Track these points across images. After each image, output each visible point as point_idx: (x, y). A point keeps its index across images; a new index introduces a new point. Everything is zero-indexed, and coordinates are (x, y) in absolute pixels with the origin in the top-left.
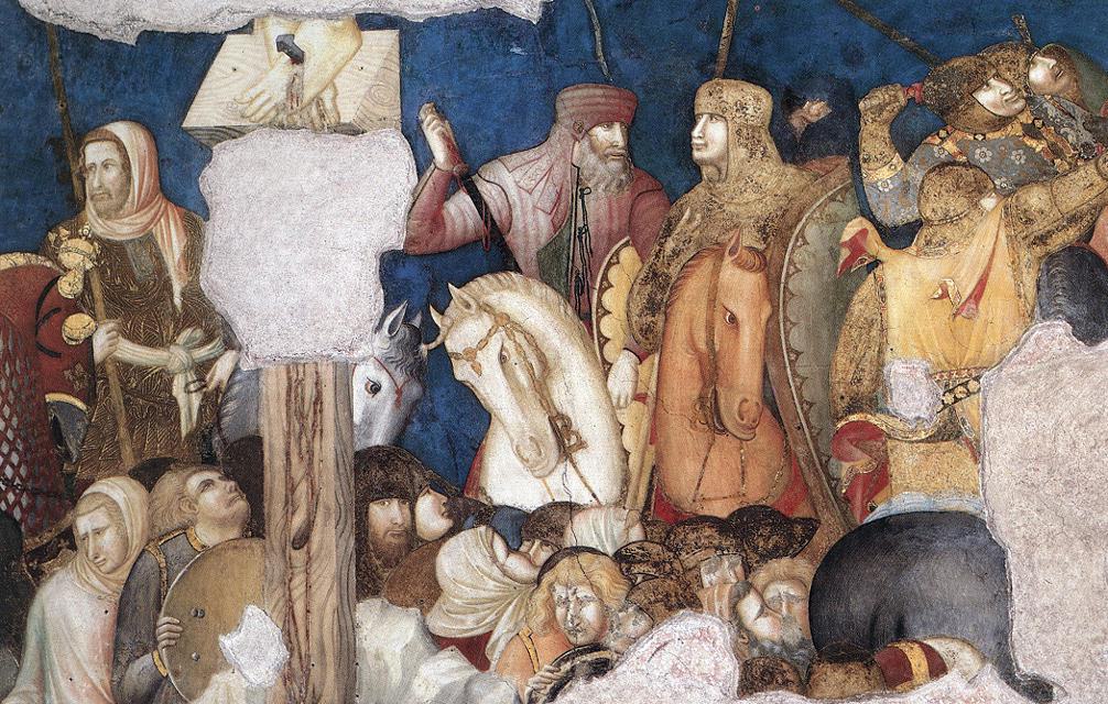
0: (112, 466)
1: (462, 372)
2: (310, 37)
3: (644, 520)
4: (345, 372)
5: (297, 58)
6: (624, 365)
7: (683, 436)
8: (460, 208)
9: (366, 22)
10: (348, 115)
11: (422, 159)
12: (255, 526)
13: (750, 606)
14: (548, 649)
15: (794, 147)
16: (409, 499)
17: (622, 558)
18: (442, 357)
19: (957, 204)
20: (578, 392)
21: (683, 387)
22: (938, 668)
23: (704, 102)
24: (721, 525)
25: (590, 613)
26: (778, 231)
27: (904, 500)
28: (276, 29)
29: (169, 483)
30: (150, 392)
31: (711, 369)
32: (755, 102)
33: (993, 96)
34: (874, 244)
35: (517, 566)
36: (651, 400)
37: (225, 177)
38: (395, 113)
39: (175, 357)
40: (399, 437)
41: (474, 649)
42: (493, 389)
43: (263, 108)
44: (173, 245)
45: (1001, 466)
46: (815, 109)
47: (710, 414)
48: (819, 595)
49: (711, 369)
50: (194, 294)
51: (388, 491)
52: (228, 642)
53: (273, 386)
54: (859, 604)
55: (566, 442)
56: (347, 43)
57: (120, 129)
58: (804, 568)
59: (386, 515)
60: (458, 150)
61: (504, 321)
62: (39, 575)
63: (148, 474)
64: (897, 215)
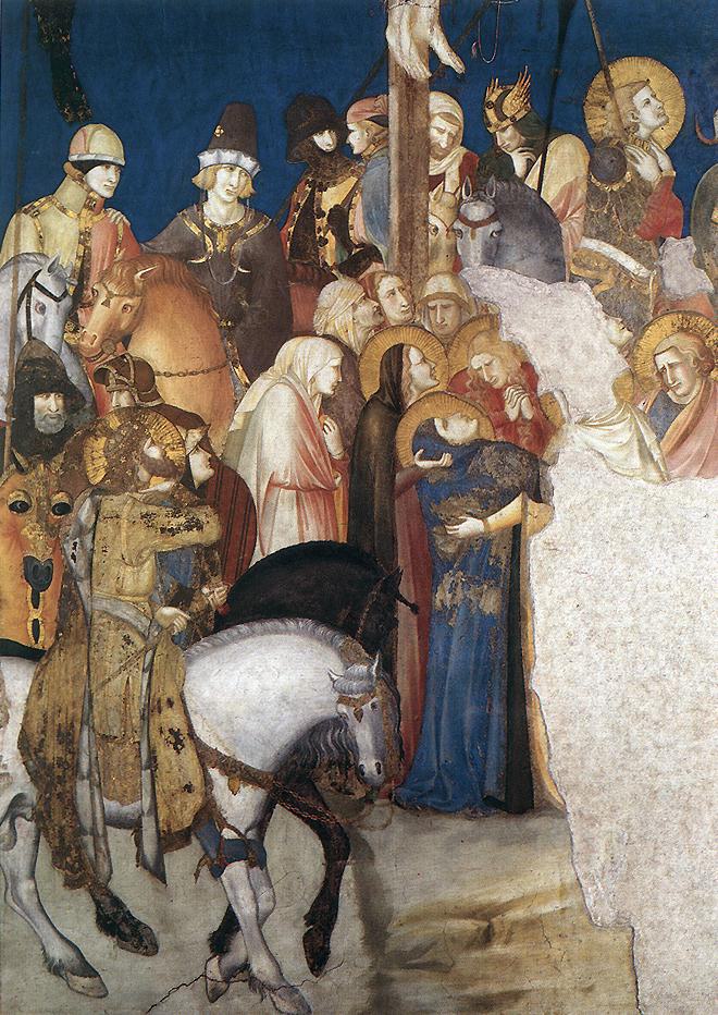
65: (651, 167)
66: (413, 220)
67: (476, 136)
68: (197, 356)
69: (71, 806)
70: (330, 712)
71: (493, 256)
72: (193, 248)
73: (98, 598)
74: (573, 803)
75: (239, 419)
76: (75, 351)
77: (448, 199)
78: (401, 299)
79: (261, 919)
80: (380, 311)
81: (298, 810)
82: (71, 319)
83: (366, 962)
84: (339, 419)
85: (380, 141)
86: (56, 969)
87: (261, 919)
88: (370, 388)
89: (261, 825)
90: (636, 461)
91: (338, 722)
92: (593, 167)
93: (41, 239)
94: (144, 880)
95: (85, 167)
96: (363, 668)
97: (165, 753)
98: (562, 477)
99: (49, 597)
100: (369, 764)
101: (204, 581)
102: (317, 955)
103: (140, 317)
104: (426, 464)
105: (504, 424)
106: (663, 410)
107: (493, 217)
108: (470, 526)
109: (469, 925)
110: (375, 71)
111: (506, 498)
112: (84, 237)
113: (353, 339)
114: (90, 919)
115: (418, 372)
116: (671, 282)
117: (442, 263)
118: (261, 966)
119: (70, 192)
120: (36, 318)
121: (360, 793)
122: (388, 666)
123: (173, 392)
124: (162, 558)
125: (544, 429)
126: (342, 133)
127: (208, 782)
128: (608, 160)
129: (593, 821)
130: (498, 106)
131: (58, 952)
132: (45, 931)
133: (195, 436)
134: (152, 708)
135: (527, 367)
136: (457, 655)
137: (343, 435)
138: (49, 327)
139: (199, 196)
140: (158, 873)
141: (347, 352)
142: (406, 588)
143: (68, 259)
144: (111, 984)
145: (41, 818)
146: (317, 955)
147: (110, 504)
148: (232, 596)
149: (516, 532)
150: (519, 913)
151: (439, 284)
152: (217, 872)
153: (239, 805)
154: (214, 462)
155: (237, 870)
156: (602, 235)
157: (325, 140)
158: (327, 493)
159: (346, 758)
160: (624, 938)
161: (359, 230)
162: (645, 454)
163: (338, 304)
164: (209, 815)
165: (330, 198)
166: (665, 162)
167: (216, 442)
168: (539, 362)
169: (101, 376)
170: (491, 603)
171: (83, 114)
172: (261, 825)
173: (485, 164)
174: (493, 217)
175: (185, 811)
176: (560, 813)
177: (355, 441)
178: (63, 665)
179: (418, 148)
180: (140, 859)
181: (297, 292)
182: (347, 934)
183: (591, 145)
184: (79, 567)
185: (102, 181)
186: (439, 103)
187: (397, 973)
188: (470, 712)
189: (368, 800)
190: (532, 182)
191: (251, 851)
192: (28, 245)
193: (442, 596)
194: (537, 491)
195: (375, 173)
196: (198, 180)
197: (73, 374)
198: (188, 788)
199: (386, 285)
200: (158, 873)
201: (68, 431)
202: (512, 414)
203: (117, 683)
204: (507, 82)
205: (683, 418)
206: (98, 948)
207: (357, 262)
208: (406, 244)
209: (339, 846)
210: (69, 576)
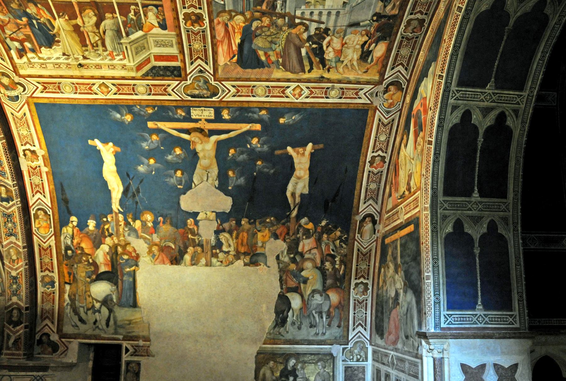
0: (191, 246)
1: (221, 240)
2: (208, 213)
3: (236, 252)
4: (211, 240)
5: (207, 214)
6: (235, 241)
7: (240, 246)
8: (221, 227)
9: (213, 212)
10: (211, 219)
11: (218, 223)
12: (203, 251)
13: (245, 260)
14: (228, 262)
15: (250, 224)
16: (216, 250)
17: (234, 255)
18: (219, 239)
19: (264, 229)
20: (231, 242)
21: (240, 241)
22: (260, 265)
23: (242, 219)
24: (242, 253)
25: (231, 259)
26: (248, 231)
27: (258, 252)
28: (205, 212)
29: (196, 248)
30: (194, 240)
31: (242, 241)
32: (247, 220)
33: (268, 220)
34: (257, 232)
35: (225, 256)
36: (237, 243)
37: (200, 223)
38: (215, 219)
39: (196, 238)
40: (215, 245)
41: (221, 262)
42: (223, 241)
43: (203, 218)
44: (196, 229)
45: (267, 249)
46: (252, 221)
47: (242, 244)
48: (251, 259)
49: (242, 241)
50: (198, 233)
51: (214, 249)
52: (201, 260)
53: (205, 241)
54: (254, 260)
55: (230, 246)
56: (211, 213)
57: (191, 219)
58: (250, 257)
59: (214, 251)
60: (221, 222)
61: (224, 236)
62: (184, 255)
63: (194, 247)
64: (259, 229)
65: (150, 224)
66: (118, 231)
67: (125, 219)
68: (90, 247)
69: (75, 304)
70: (109, 293)
71: (129, 235)
72: (87, 233)
73: (78, 277)
74: (142, 306)
75: (95, 255)
76: (73, 245)
77: (122, 228)
78: (117, 240)
79: (100, 320)
80: (114, 241)
81: (105, 306)
82: (72, 242)
83: (114, 326)
84: (109, 255)
85: (112, 220)
86: (73, 326)
87: (100, 320)
88: (113, 251)
89: (100, 308)
90: (150, 262)
91: (110, 295)
92: (142, 224)
93: (67, 231)
94: (85, 315)
95: (72, 222)
96: (114, 288)
97: (87, 298)
98: (140, 264)
99: (72, 276)
100: (115, 300)
101: (92, 275)
102: (107, 325)
103: (81, 241)
104: (121, 261)
105: (132, 256)
106: (154, 256)
107: (129, 230)
108: (128, 270)
109: (128, 322)
110: (111, 211)
111: (132, 266)
112: (73, 231)
113: (111, 245)
114: (77, 319)
115: (120, 249)
116: (154, 239)
117: (122, 236)
118: (100, 326)
119: (70, 225)
120: (67, 241)
121: (113, 304)
122: (117, 287)
123: (87, 251)
124: (86, 272)
125: (138, 256)
126: (107, 218)
127: (93, 302)
128: (144, 224)
129: (145, 309)
130: (128, 216)
131: (73, 324)
132: (72, 321)
133: (90, 257)
134: (86, 292)
135: (134, 249)
136: (126, 286)
137: (110, 257)
138: (69, 242)
139: (88, 226)
140: (86, 313)
141: (110, 246)
142: (120, 277)
143: (71, 233)
144: (80, 328)
145: (71, 306)
146: (107, 325)
147: (79, 265)
148: (96, 278)
149: (134, 271)
150: (134, 321)
151: (122, 238)
152: (94, 314)
153: (97, 305)
154: (93, 260)
155: (97, 314)
156: (144, 233)
157: (105, 219)
158: (108, 265)
159: (112, 300)
160: (148, 325)
161: (110, 231)
162: (152, 261)
163: (108, 240)
164: (93, 306)
165: (106, 227)
166: (152, 224)
167: (93, 258)
168: (136, 249)
169: (76, 249)
170: (131, 280)
171: (71, 214)
172: (100, 308)
173: (127, 224)
174: (129, 230)
175: (90, 306)
176: (140, 308)
177: (112, 259)
178: (74, 285)
179: (118, 221)
180: (84, 312)
181: (102, 239)
182: (112, 322)
183: (142, 221)
184: (75, 273)
185: (75, 224)
186: (120, 215)
187: (118, 328)
188: (128, 294)
189: (115, 305)
190: (134, 226)
191: (99, 311)
192: (65, 231)
193: (124, 278)
194: (137, 265)
195: (112, 224)
196: (88, 224)
197: (73, 248)
198: (91, 303)
199: (115, 238)
200: (86, 313)
201: (72, 256)
202: (133, 255)
203: (81, 288)
204: (130, 213)
205: (156, 257)
206: (79, 323)
207: (110, 235)
208: (117, 233)
209: (111, 311)
210: (74, 274)
